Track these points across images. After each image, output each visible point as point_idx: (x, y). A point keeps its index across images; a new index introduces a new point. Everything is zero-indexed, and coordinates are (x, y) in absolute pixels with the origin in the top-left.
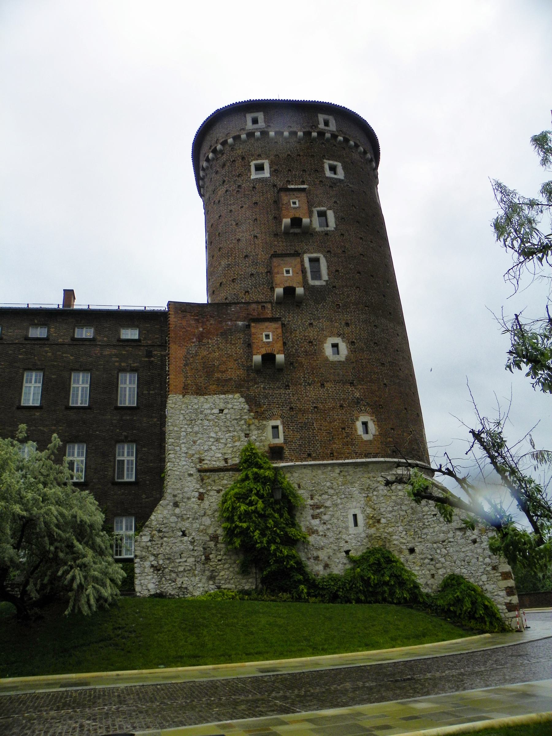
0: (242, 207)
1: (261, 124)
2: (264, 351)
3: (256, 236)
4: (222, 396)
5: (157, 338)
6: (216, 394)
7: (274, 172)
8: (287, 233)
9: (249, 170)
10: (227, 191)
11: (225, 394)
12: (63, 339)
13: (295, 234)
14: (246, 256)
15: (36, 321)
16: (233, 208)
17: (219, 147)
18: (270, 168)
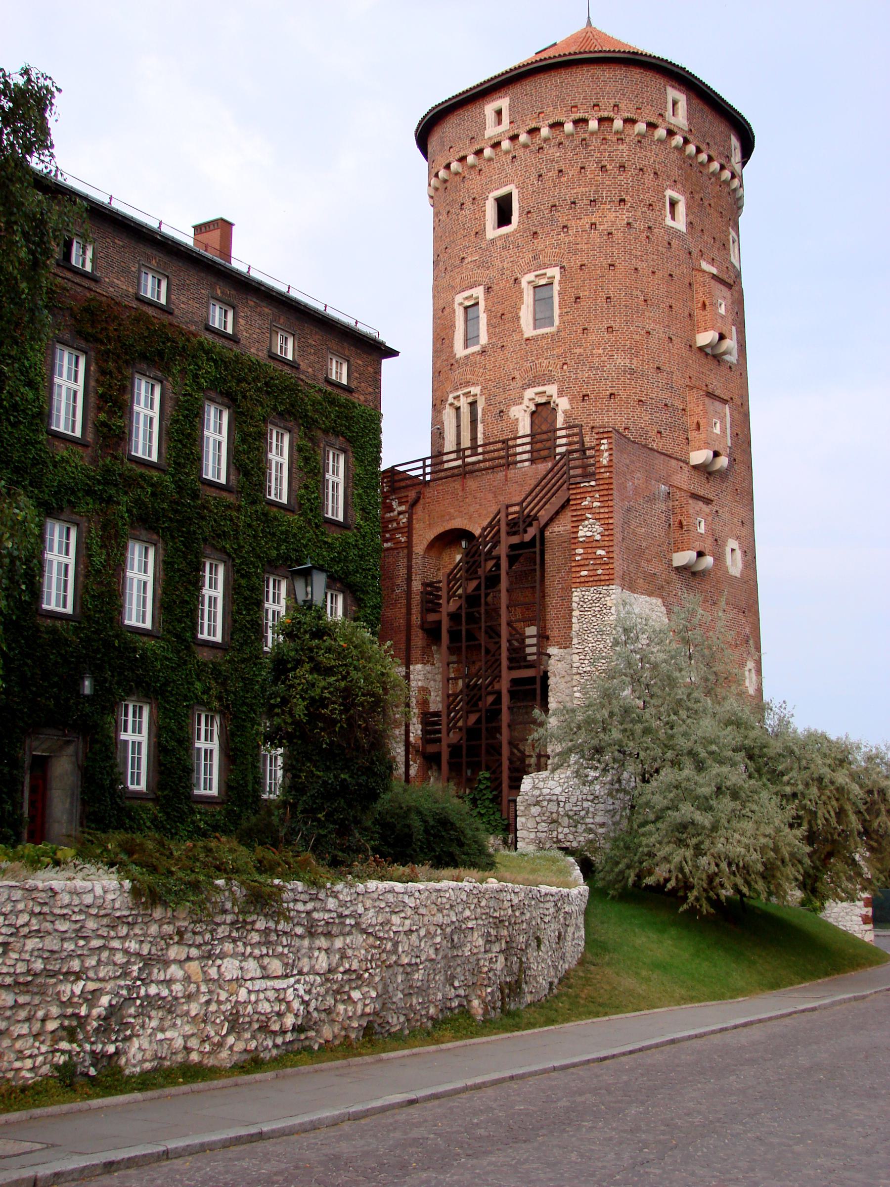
0: (653, 272)
1: (680, 119)
2: (699, 545)
3: (670, 339)
4: (648, 599)
5: (370, 394)
6: (642, 594)
7: (690, 224)
8: (701, 349)
9: (664, 206)
10: (629, 224)
11: (649, 596)
12: (258, 350)
13: (707, 354)
14: (658, 368)
15: (219, 292)
16: (640, 265)
17: (618, 124)
18: (687, 215)
